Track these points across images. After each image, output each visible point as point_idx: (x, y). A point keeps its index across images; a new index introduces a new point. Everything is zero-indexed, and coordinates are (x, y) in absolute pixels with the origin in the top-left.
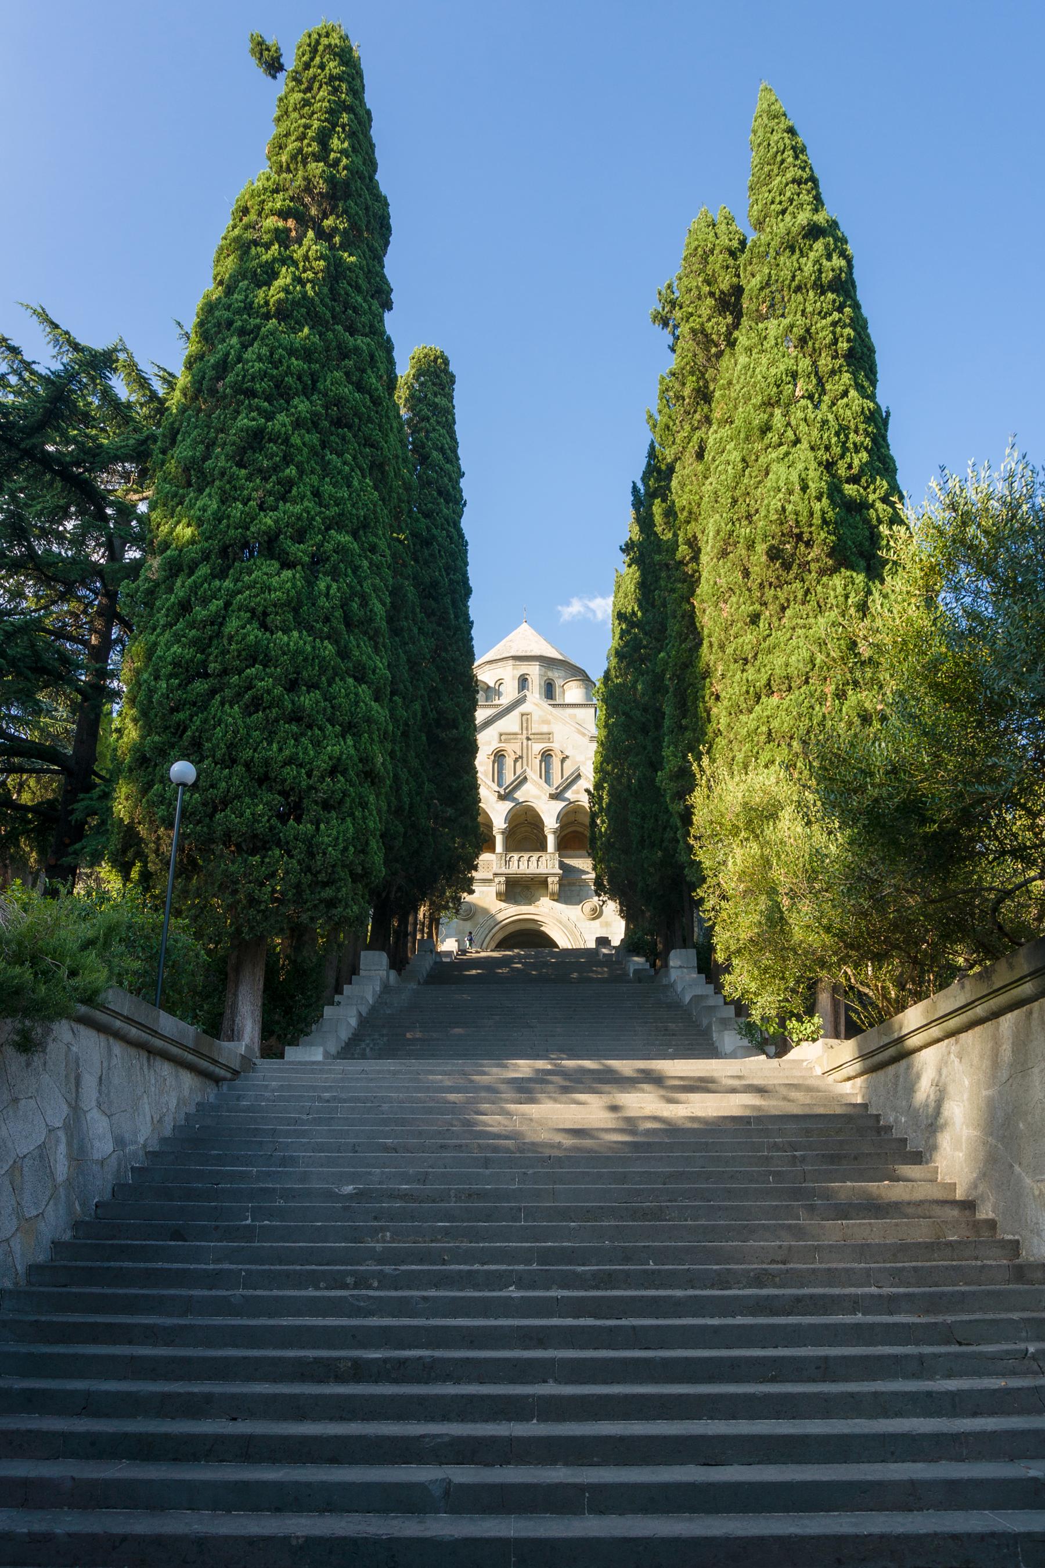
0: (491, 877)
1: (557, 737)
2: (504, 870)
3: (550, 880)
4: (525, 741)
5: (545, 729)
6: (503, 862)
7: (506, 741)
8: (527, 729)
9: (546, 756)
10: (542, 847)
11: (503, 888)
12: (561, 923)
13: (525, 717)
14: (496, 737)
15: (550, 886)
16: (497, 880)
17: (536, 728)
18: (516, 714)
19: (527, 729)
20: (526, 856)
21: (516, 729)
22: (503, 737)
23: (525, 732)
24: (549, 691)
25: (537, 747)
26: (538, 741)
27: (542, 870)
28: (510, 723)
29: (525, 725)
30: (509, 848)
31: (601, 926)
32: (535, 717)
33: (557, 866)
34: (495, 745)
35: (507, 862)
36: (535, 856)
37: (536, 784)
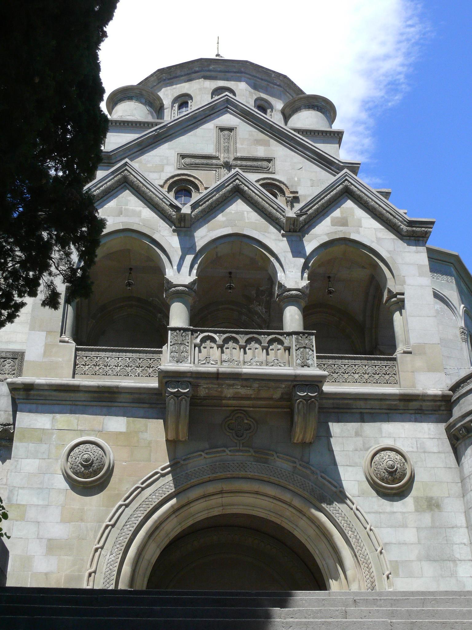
0: (154, 384)
5: (260, 152)
18: (209, 129)
22: (188, 160)
30: (199, 319)
31: (418, 510)
34: (171, 170)
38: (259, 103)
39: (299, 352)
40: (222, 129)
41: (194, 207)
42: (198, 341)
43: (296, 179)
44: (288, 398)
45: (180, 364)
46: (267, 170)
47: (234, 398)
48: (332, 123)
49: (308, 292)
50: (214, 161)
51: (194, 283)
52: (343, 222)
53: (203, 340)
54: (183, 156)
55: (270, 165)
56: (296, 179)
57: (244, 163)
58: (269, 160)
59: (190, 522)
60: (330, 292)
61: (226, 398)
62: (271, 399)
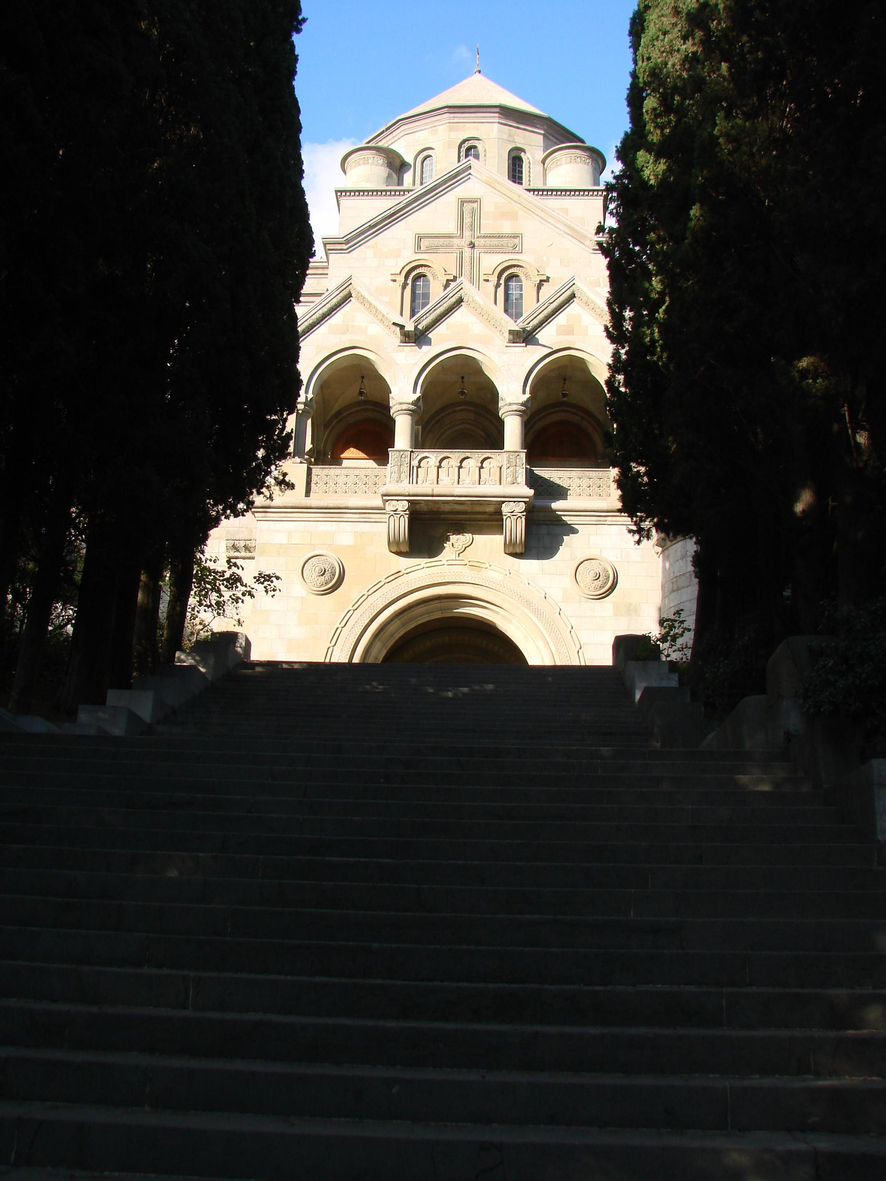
0: (379, 503)
1: (528, 243)
2: (406, 487)
3: (505, 509)
4: (467, 251)
5: (507, 228)
6: (405, 468)
7: (430, 250)
8: (472, 228)
9: (508, 277)
10: (495, 441)
11: (404, 523)
12: (528, 604)
13: (467, 207)
14: (411, 242)
15: (507, 523)
16: (389, 507)
17: (488, 226)
18: (448, 201)
19: (472, 228)
20: (456, 456)
21: (451, 227)
23: (467, 233)
24: (515, 167)
25: (491, 262)
26: (491, 250)
27: (490, 488)
28: (440, 216)
29: (467, 220)
32: (487, 207)
33: (522, 478)
34: (408, 256)
35: (413, 472)
36: (477, 455)
37: (480, 312)
38: (514, 154)
39: (509, 470)
40: (463, 202)
41: (418, 322)
42: (415, 463)
43: (545, 258)
44: (499, 513)
45: (400, 485)
46: (514, 249)
47: (452, 513)
48: (601, 173)
49: (529, 405)
50: (456, 241)
51: (418, 399)
52: (568, 330)
53: (420, 462)
54: (420, 238)
55: (517, 241)
56: (545, 258)
57: (488, 241)
58: (515, 237)
59: (413, 625)
60: (564, 395)
61: (444, 513)
62: (485, 513)
